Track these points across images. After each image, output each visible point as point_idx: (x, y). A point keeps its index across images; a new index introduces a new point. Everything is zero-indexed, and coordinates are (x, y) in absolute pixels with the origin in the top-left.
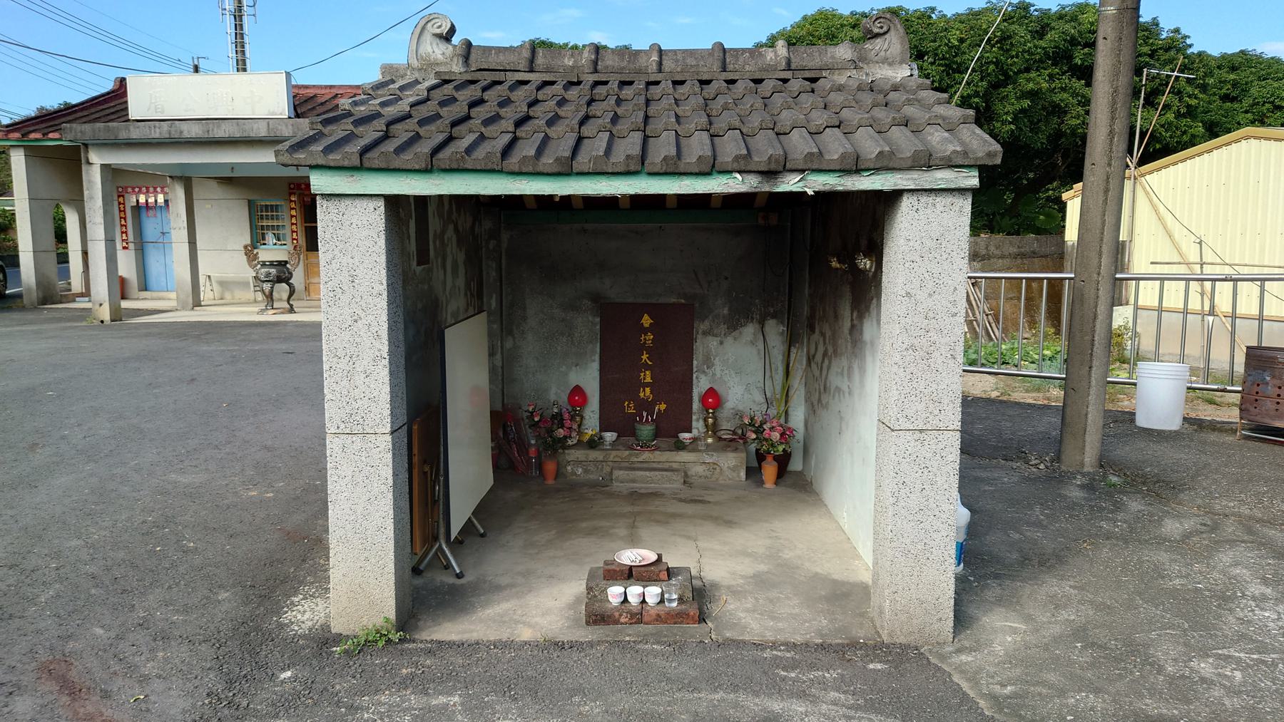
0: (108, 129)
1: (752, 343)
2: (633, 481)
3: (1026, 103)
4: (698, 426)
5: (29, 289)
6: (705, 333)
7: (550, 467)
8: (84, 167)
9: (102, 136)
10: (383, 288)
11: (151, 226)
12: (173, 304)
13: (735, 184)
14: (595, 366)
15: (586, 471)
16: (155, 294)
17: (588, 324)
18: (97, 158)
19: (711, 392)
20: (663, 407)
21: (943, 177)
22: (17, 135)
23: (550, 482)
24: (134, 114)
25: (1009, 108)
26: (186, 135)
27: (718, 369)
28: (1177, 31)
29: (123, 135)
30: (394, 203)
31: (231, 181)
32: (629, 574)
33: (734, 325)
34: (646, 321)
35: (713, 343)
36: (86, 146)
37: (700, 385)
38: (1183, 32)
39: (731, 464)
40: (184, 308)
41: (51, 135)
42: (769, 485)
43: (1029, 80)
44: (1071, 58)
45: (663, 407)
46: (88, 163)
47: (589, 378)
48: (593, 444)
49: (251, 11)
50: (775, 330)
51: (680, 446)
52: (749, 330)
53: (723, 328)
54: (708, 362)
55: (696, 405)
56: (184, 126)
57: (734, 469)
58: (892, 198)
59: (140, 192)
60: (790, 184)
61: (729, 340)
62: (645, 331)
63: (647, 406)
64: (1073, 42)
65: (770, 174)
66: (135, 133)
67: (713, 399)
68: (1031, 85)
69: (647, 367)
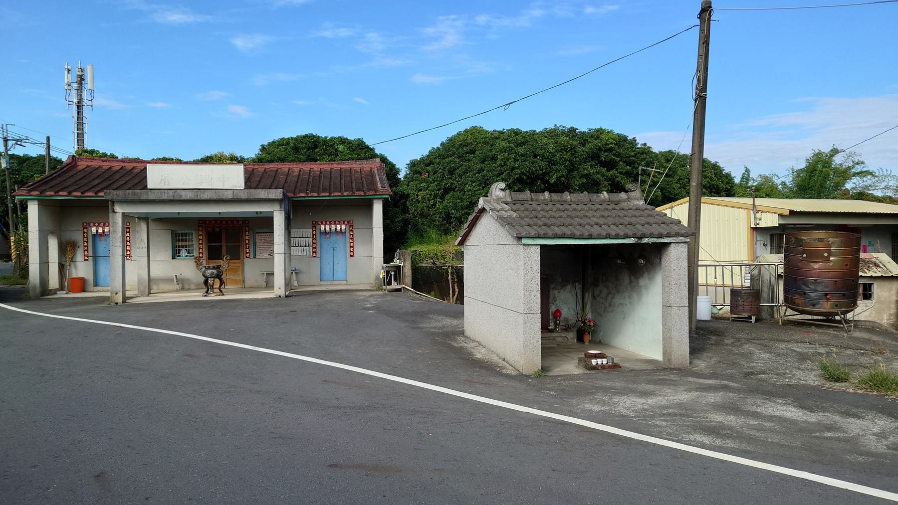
0: (134, 194)
3: (584, 180)
5: (34, 287)
8: (111, 215)
9: (130, 197)
10: (539, 271)
11: (101, 246)
12: (136, 292)
13: (632, 241)
16: (105, 288)
18: (119, 209)
21: (681, 239)
22: (37, 193)
24: (150, 185)
25: (577, 183)
26: (184, 197)
28: (645, 144)
29: (144, 197)
30: (542, 246)
31: (162, 220)
32: (596, 356)
33: (563, 286)
35: (556, 292)
36: (113, 202)
38: (648, 145)
40: (142, 295)
41: (61, 193)
43: (584, 169)
44: (599, 157)
46: (114, 212)
49: (89, 103)
50: (579, 287)
52: (569, 287)
54: (555, 300)
56: (183, 193)
57: (572, 339)
58: (667, 245)
59: (99, 226)
60: (645, 241)
61: (562, 291)
64: (600, 149)
65: (640, 238)
66: (151, 196)
68: (586, 172)
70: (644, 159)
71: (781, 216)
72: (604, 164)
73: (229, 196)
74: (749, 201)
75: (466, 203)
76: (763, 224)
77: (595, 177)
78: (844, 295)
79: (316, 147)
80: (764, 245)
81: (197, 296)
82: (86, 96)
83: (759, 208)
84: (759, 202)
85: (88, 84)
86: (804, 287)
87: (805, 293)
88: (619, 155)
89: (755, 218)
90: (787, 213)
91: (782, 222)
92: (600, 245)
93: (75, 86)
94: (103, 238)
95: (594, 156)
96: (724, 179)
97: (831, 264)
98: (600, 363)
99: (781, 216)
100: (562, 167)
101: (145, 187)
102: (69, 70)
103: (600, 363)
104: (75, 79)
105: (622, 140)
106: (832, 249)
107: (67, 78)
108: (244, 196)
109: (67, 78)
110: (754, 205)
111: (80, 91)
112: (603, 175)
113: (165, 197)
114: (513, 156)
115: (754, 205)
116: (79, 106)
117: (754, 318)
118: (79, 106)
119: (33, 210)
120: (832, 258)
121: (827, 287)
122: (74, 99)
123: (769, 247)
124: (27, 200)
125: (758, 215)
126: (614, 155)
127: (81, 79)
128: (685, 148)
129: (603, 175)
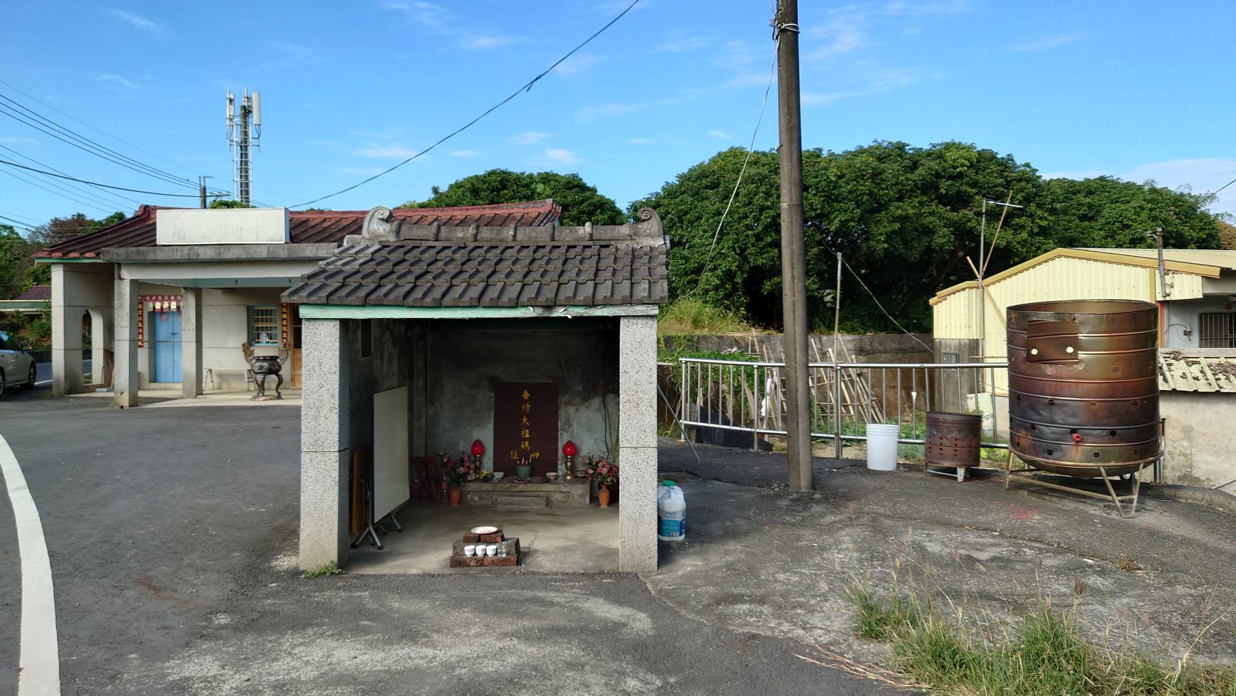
0: (139, 253)
1: (598, 410)
2: (512, 504)
3: (897, 226)
4: (562, 469)
5: (58, 381)
6: (566, 404)
7: (455, 494)
8: (116, 282)
9: (134, 257)
10: (337, 369)
11: (163, 328)
12: (180, 393)
13: (530, 312)
14: (490, 427)
15: (481, 498)
16: (163, 385)
17: (486, 397)
18: (127, 275)
19: (570, 444)
20: (537, 455)
21: (640, 310)
22: (59, 254)
23: (455, 505)
24: (160, 240)
25: (882, 230)
26: (202, 257)
27: (575, 427)
28: (1027, 165)
29: (151, 257)
30: (345, 323)
31: (234, 291)
32: (479, 539)
33: (585, 398)
34: (526, 395)
35: (572, 410)
36: (119, 265)
37: (563, 439)
38: (1034, 166)
39: (579, 492)
40: (188, 397)
41: (87, 255)
42: (604, 506)
43: (898, 208)
44: (937, 188)
45: (537, 455)
46: (120, 279)
47: (486, 435)
48: (487, 479)
49: (256, 142)
51: (548, 481)
52: (596, 402)
53: (578, 399)
54: (568, 423)
55: (560, 454)
56: (201, 250)
57: (582, 496)
58: (616, 320)
59: (157, 300)
60: (559, 312)
61: (583, 408)
62: (525, 402)
63: (526, 454)
64: (938, 176)
65: (549, 307)
66: (161, 255)
67: (572, 449)
68: (899, 212)
69: (526, 427)
70: (1022, 190)
71: (1207, 279)
72: (943, 200)
73: (263, 254)
74: (1153, 253)
75: (692, 265)
76: (1176, 295)
77: (926, 221)
78: (1113, 433)
79: (504, 187)
80: (1187, 333)
81: (245, 400)
82: (252, 132)
83: (1168, 266)
84: (1171, 254)
85: (254, 118)
86: (1031, 414)
87: (1033, 427)
88: (974, 184)
89: (1164, 285)
90: (1216, 273)
91: (1211, 290)
92: (471, 320)
93: (238, 120)
94: (164, 317)
95: (928, 187)
96: (1196, 223)
97: (1081, 367)
98: (479, 553)
99: (1207, 279)
100: (852, 205)
101: (153, 243)
102: (231, 101)
103: (479, 553)
104: (239, 112)
105: (985, 160)
106: (1081, 336)
107: (229, 110)
108: (283, 254)
109: (229, 110)
110: (1160, 260)
111: (245, 125)
112: (941, 218)
113: (177, 256)
114: (763, 189)
115: (1160, 260)
116: (244, 146)
117: (961, 473)
118: (244, 146)
119: (57, 276)
120: (1082, 355)
121: (1074, 415)
122: (237, 137)
123: (1196, 337)
124: (49, 266)
125: (1168, 279)
126: (967, 184)
127: (247, 112)
128: (764, 137)
129: (941, 218)
